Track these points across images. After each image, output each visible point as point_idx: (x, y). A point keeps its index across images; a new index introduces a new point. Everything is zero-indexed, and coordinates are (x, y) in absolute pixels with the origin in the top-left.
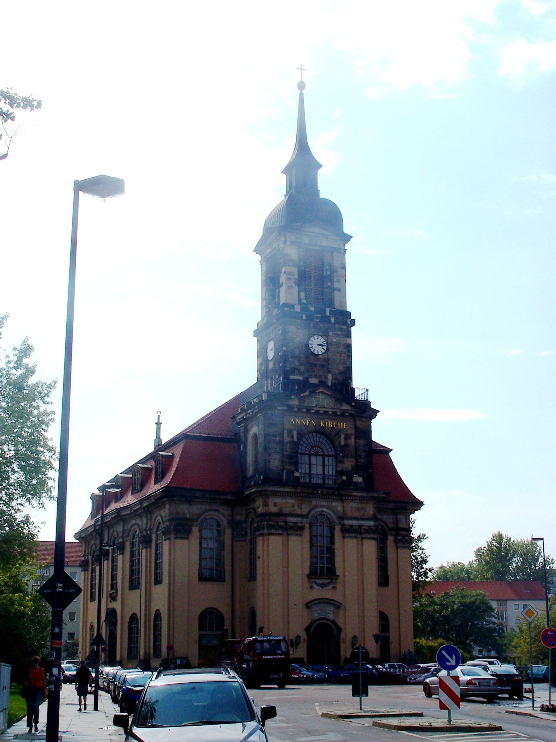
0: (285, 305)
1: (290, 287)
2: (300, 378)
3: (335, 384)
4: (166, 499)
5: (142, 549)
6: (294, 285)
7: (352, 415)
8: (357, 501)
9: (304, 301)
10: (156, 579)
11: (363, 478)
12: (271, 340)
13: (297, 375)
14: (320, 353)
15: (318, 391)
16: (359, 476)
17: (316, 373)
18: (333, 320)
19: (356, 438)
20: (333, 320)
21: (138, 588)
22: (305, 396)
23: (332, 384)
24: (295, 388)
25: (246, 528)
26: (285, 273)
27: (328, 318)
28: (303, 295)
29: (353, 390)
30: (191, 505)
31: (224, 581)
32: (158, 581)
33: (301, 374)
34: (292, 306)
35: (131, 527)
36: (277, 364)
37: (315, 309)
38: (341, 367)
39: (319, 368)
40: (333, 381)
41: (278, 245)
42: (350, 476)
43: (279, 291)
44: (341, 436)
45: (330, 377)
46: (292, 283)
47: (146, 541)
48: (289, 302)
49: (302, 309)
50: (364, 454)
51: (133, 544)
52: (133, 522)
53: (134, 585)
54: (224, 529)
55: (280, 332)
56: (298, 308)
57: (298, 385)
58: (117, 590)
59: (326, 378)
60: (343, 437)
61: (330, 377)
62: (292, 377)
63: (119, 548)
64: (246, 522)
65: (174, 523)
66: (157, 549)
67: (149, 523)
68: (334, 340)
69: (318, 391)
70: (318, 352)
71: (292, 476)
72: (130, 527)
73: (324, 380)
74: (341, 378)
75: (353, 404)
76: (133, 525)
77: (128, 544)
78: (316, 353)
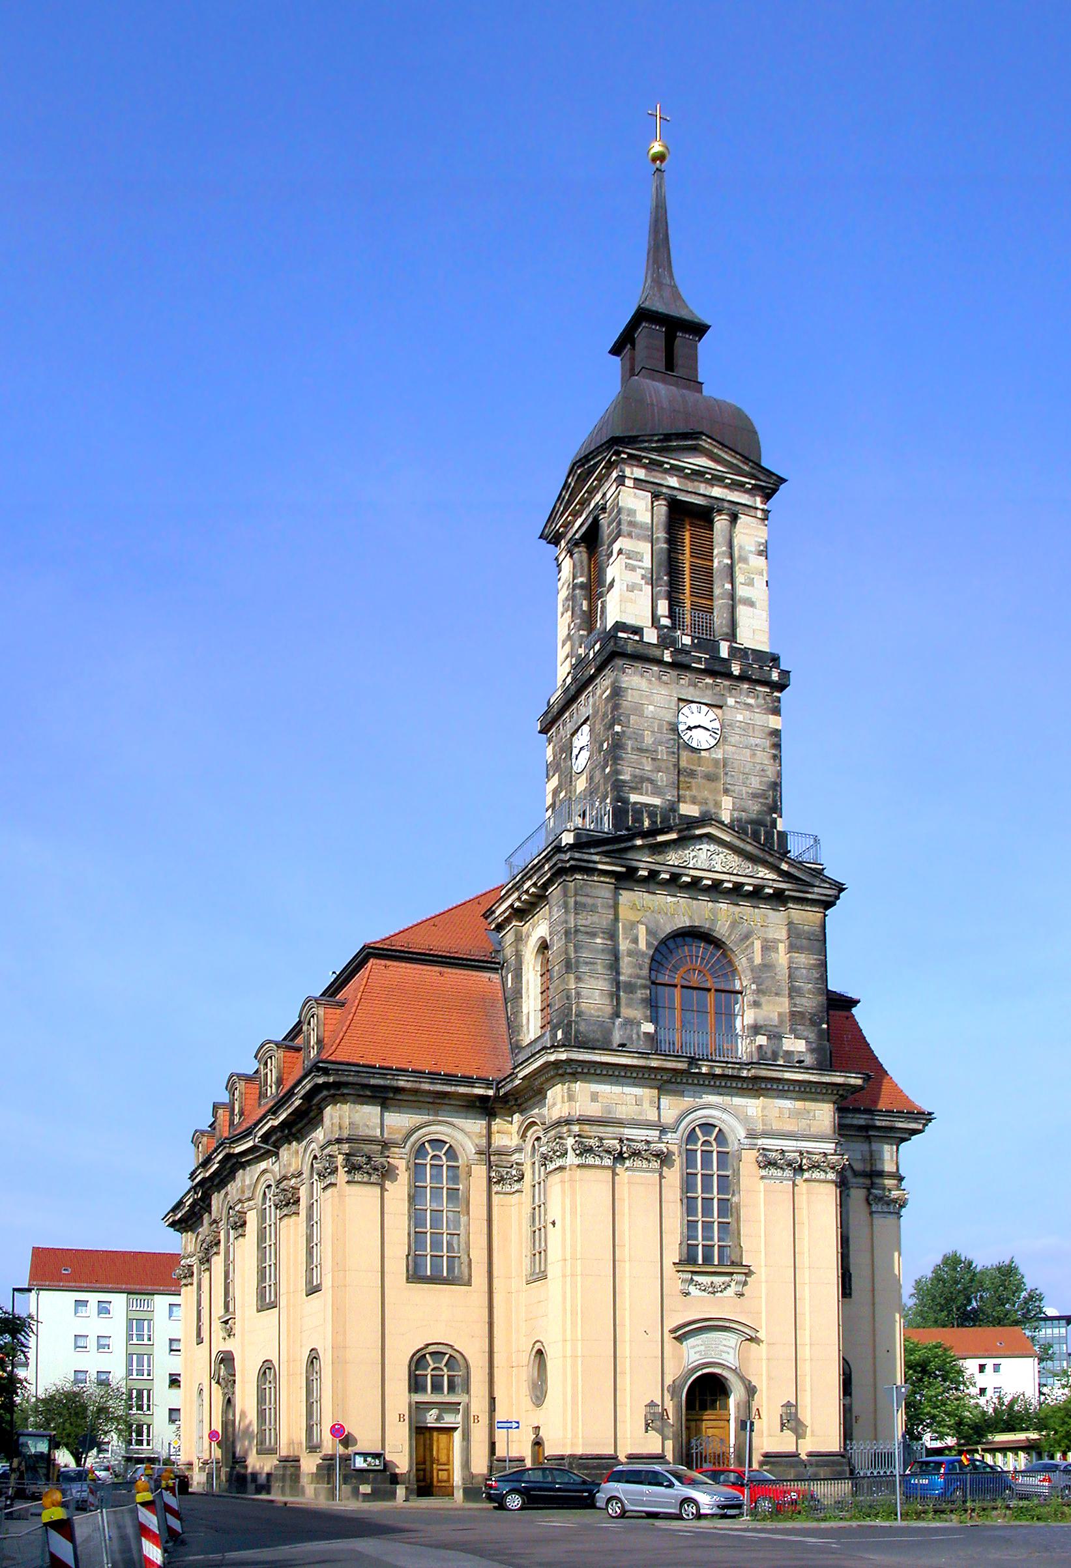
2: (657, 801)
3: (739, 820)
6: (643, 582)
13: (647, 794)
28: (663, 607)
29: (783, 836)
33: (657, 792)
37: (692, 641)
40: (736, 814)
57: (652, 816)
59: (718, 805)
60: (758, 945)
61: (727, 802)
62: (634, 798)
68: (740, 718)
75: (784, 867)
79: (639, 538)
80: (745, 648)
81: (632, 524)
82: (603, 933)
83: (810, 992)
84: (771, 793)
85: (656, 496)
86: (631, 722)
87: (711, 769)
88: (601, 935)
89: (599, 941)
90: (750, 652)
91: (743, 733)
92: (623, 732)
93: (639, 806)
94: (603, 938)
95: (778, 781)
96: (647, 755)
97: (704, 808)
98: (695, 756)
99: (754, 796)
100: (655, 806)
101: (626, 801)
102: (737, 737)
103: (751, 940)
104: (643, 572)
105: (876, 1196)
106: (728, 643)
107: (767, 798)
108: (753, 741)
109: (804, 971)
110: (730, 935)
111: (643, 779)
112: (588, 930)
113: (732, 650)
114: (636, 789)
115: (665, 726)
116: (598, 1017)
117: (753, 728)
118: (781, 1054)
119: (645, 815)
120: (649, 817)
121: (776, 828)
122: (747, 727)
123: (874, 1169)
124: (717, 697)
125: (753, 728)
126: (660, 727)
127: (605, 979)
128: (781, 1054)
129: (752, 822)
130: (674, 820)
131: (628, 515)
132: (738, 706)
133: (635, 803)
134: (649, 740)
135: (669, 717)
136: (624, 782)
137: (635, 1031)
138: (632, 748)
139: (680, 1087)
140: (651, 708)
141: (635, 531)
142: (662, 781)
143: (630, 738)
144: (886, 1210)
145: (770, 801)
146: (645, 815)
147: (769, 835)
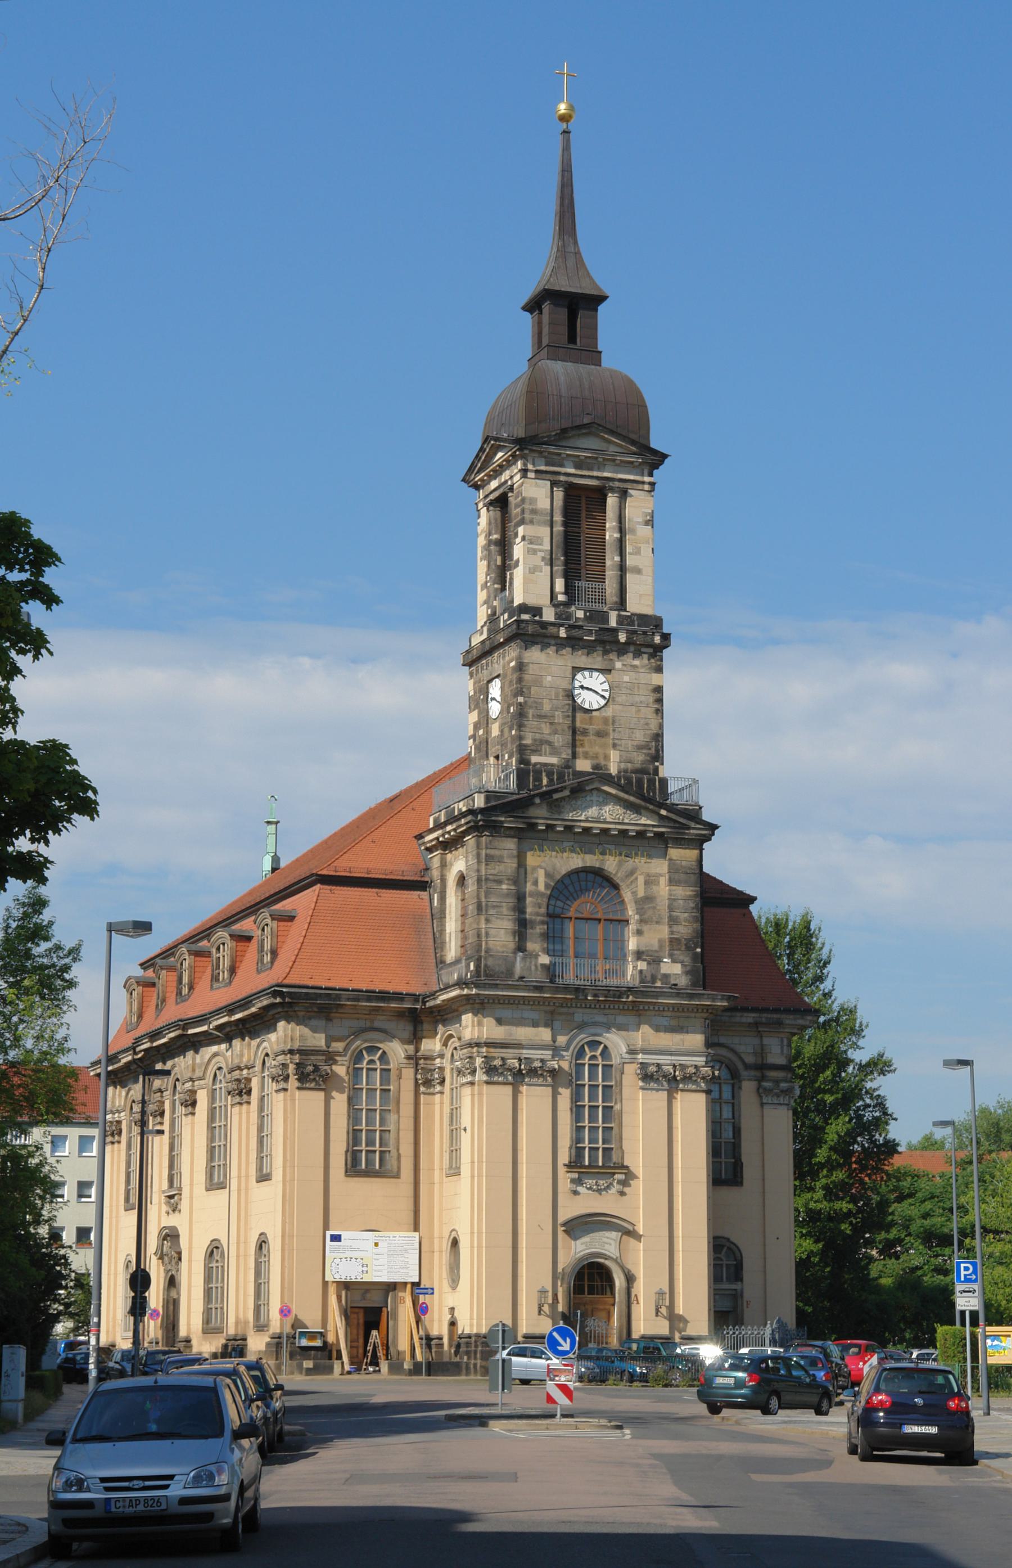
0: (524, 608)
1: (533, 570)
2: (554, 760)
3: (626, 771)
4: (280, 1010)
5: (232, 1105)
6: (543, 563)
7: (659, 835)
8: (669, 1014)
9: (561, 598)
10: (260, 1168)
11: (683, 966)
12: (498, 676)
13: (545, 755)
14: (595, 706)
15: (587, 788)
16: (674, 961)
17: (587, 749)
18: (622, 637)
19: (671, 882)
20: (622, 637)
21: (225, 1188)
22: (563, 799)
23: (619, 772)
24: (541, 781)
25: (442, 1069)
26: (524, 538)
27: (614, 631)
28: (560, 585)
29: (664, 782)
30: (331, 1020)
31: (397, 1176)
32: (264, 1177)
33: (554, 752)
34: (537, 611)
35: (210, 1060)
36: (506, 730)
37: (585, 614)
38: (640, 736)
39: (592, 737)
40: (623, 766)
41: (511, 477)
42: (656, 961)
43: (511, 575)
44: (636, 879)
45: (614, 756)
46: (537, 560)
47: (242, 1091)
48: (532, 601)
49: (558, 616)
50: (686, 915)
51: (212, 1098)
52: (214, 1048)
53: (215, 1181)
54: (400, 1070)
55: (513, 664)
56: (549, 615)
57: (550, 774)
58: (180, 1189)
59: (607, 757)
60: (641, 880)
61: (614, 756)
62: (535, 759)
63: (185, 1104)
64: (442, 1056)
65: (297, 1058)
66: (261, 1108)
67: (246, 1052)
68: (626, 678)
69: (587, 788)
70: (591, 703)
71: (533, 963)
72: (207, 1057)
73: (603, 763)
74: (639, 758)
75: (663, 812)
76: (216, 1055)
77: (202, 1098)
78: (587, 706)
79: (539, 524)
80: (632, 614)
81: (534, 511)
82: (508, 879)
83: (686, 920)
84: (654, 744)
85: (554, 484)
86: (532, 692)
87: (601, 727)
88: (506, 882)
89: (504, 887)
90: (635, 618)
91: (629, 692)
92: (525, 702)
93: (538, 766)
94: (507, 884)
95: (660, 733)
96: (546, 720)
97: (595, 762)
98: (587, 716)
99: (639, 748)
100: (552, 765)
101: (527, 762)
102: (624, 697)
103: (635, 876)
104: (542, 554)
105: (765, 1089)
106: (617, 612)
107: (650, 749)
108: (637, 699)
109: (681, 902)
110: (617, 872)
111: (542, 742)
112: (496, 878)
113: (621, 620)
114: (537, 751)
115: (561, 693)
116: (503, 952)
117: (638, 688)
118: (659, 977)
119: (544, 774)
120: (547, 776)
121: (658, 775)
122: (632, 686)
123: (765, 1062)
124: (606, 662)
125: (638, 688)
126: (557, 695)
127: (509, 920)
128: (659, 977)
129: (636, 771)
130: (568, 776)
131: (530, 504)
132: (625, 668)
133: (536, 764)
134: (547, 707)
135: (565, 684)
136: (526, 746)
137: (533, 963)
138: (533, 716)
139: (571, 1010)
140: (549, 678)
141: (536, 518)
142: (558, 742)
143: (531, 707)
144: (776, 1102)
145: (653, 751)
146: (544, 774)
147: (652, 782)
